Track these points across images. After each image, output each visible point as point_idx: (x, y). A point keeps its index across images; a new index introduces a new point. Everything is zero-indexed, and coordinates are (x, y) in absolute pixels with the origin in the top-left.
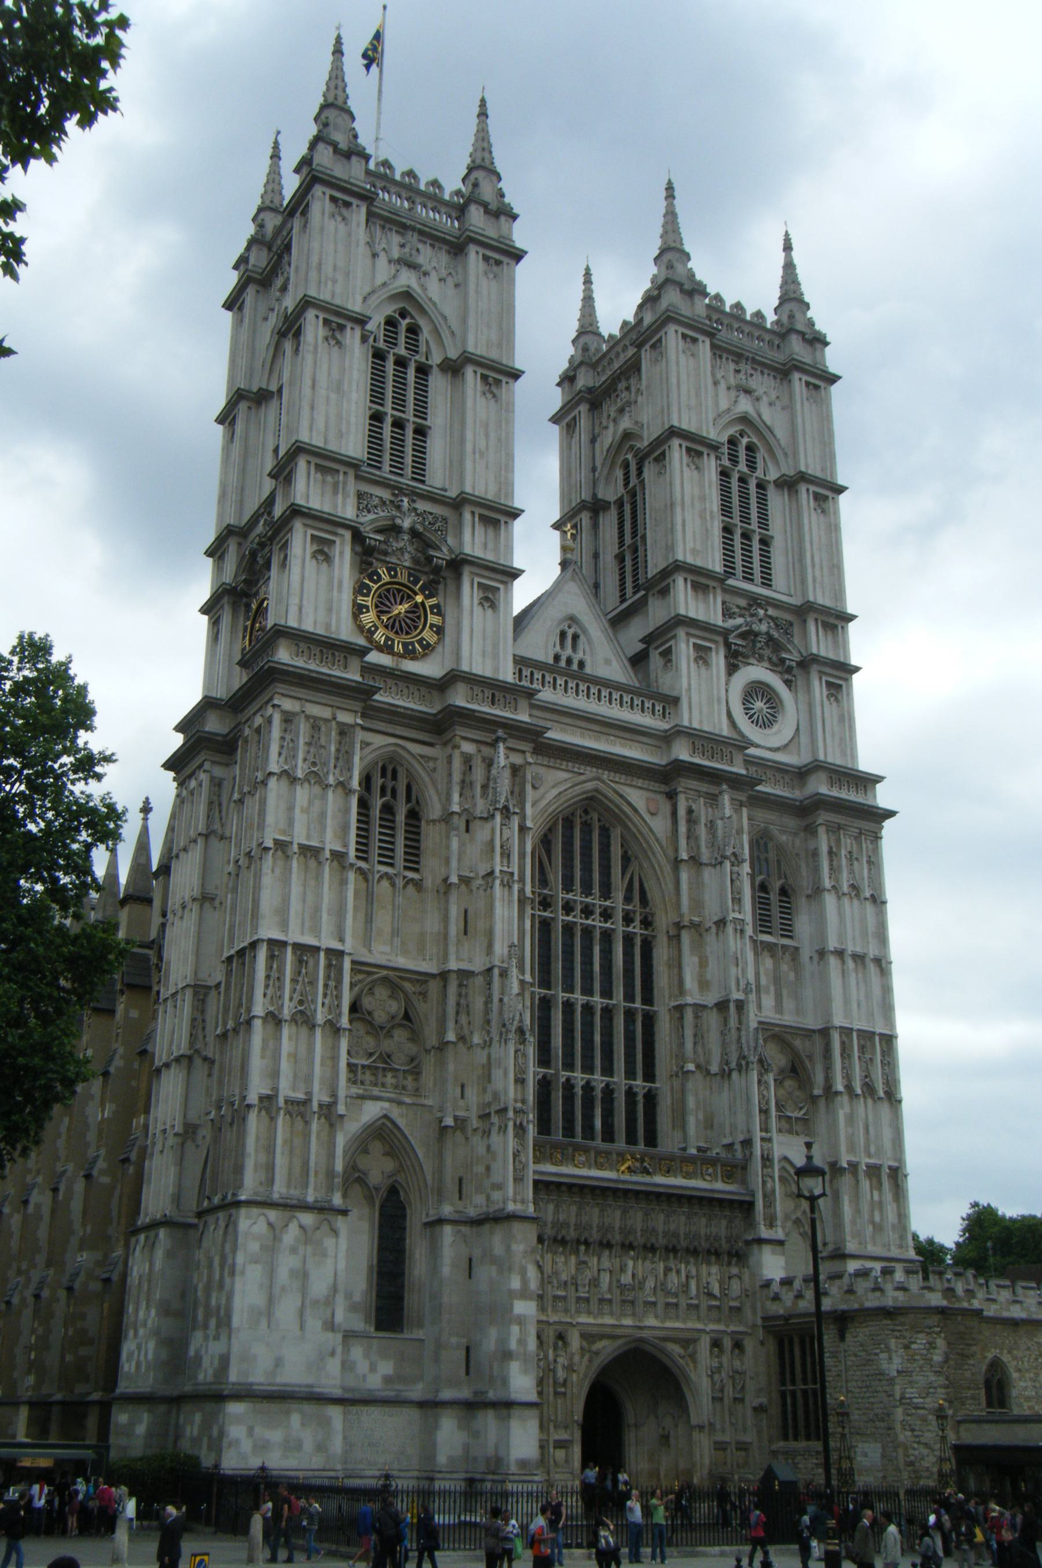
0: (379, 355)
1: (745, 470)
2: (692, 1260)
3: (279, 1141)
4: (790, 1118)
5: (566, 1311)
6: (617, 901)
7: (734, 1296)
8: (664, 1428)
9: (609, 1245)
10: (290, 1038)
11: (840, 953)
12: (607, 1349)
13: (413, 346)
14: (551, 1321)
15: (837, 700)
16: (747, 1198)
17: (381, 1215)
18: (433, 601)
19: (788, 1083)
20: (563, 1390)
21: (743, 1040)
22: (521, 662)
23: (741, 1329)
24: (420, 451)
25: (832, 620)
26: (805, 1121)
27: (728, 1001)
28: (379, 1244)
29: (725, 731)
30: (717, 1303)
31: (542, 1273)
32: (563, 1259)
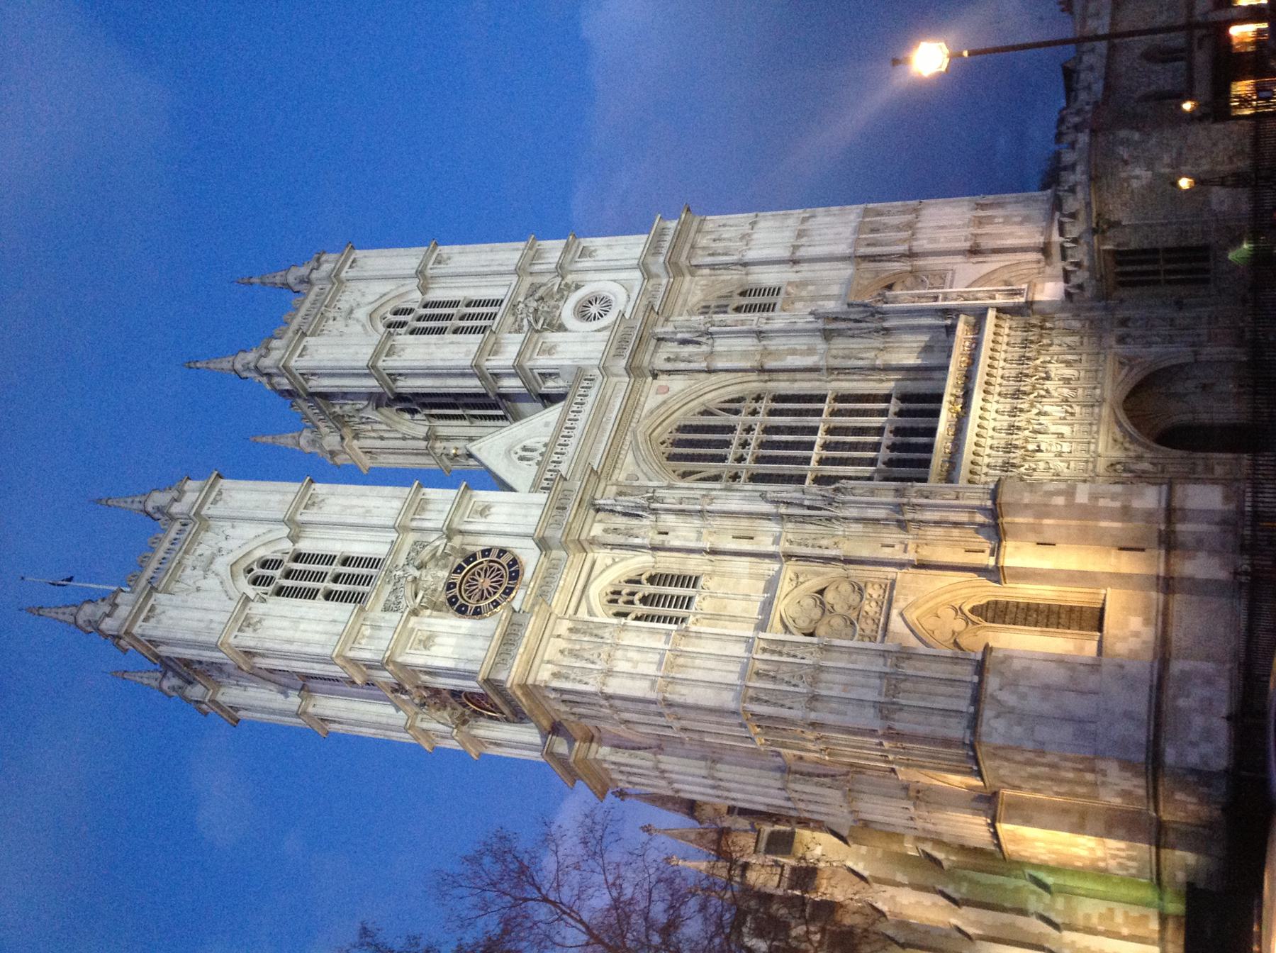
0: (280, 592)
1: (411, 315)
3: (922, 704)
6: (739, 421)
10: (831, 689)
11: (796, 247)
13: (276, 564)
15: (595, 250)
17: (993, 622)
18: (479, 555)
21: (857, 317)
22: (535, 487)
24: (359, 561)
25: (532, 253)
27: (825, 330)
28: (1021, 625)
29: (606, 333)
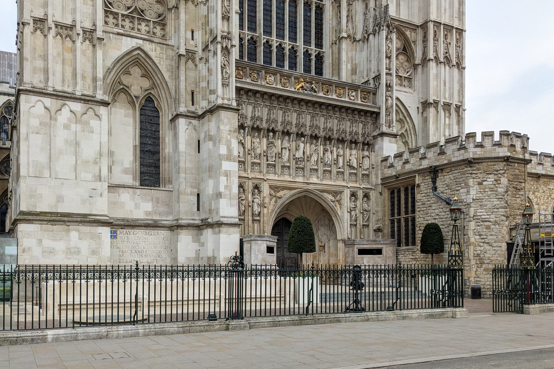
2: (340, 146)
4: (401, 77)
5: (260, 172)
7: (365, 168)
8: (322, 242)
9: (288, 134)
12: (286, 195)
14: (250, 177)
16: (376, 110)
17: (141, 115)
19: (401, 57)
20: (258, 218)
23: (369, 186)
26: (409, 79)
30: (355, 172)
31: (244, 148)
32: (258, 140)
